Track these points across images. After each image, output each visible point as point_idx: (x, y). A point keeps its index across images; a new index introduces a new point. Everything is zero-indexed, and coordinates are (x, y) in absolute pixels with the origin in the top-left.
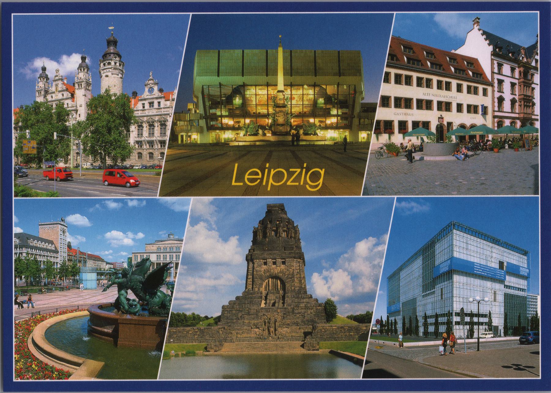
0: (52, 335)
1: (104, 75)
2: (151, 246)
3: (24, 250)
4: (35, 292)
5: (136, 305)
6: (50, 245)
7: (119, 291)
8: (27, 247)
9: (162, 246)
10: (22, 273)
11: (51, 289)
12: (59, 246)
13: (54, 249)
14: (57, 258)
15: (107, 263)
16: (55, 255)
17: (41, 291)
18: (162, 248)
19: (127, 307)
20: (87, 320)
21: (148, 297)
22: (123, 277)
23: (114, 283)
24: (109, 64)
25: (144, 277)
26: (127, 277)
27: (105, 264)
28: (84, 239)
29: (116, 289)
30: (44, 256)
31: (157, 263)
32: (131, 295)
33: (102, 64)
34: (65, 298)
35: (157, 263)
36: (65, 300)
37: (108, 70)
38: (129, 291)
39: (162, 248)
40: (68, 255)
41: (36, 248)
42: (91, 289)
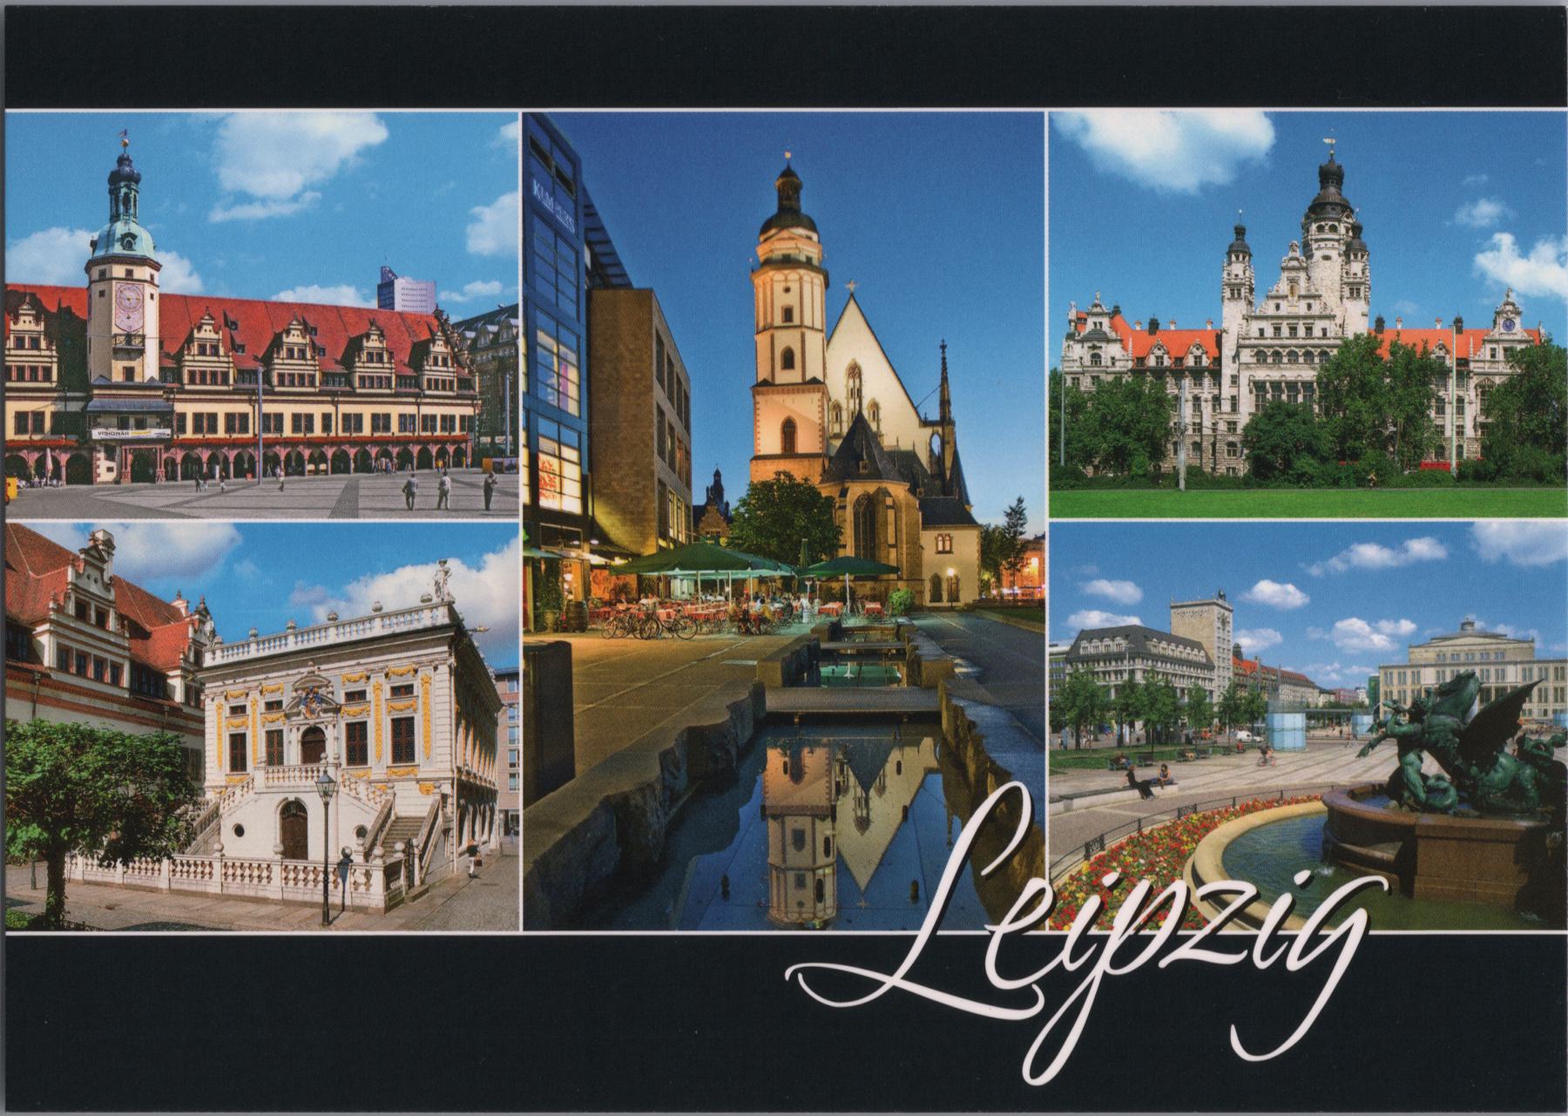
1: (1318, 255)
3: (1139, 665)
5: (1445, 791)
7: (1402, 755)
8: (1147, 656)
9: (1448, 651)
10: (1138, 715)
12: (1214, 654)
15: (1322, 692)
16: (1206, 674)
19: (1422, 795)
20: (1322, 823)
21: (1474, 770)
22: (1411, 721)
23: (1385, 737)
24: (1334, 229)
25: (1463, 720)
26: (1421, 721)
29: (1395, 750)
31: (1497, 690)
32: (1430, 766)
33: (1314, 226)
34: (1238, 772)
35: (1497, 690)
37: (1330, 244)
38: (1426, 755)
42: (1294, 750)
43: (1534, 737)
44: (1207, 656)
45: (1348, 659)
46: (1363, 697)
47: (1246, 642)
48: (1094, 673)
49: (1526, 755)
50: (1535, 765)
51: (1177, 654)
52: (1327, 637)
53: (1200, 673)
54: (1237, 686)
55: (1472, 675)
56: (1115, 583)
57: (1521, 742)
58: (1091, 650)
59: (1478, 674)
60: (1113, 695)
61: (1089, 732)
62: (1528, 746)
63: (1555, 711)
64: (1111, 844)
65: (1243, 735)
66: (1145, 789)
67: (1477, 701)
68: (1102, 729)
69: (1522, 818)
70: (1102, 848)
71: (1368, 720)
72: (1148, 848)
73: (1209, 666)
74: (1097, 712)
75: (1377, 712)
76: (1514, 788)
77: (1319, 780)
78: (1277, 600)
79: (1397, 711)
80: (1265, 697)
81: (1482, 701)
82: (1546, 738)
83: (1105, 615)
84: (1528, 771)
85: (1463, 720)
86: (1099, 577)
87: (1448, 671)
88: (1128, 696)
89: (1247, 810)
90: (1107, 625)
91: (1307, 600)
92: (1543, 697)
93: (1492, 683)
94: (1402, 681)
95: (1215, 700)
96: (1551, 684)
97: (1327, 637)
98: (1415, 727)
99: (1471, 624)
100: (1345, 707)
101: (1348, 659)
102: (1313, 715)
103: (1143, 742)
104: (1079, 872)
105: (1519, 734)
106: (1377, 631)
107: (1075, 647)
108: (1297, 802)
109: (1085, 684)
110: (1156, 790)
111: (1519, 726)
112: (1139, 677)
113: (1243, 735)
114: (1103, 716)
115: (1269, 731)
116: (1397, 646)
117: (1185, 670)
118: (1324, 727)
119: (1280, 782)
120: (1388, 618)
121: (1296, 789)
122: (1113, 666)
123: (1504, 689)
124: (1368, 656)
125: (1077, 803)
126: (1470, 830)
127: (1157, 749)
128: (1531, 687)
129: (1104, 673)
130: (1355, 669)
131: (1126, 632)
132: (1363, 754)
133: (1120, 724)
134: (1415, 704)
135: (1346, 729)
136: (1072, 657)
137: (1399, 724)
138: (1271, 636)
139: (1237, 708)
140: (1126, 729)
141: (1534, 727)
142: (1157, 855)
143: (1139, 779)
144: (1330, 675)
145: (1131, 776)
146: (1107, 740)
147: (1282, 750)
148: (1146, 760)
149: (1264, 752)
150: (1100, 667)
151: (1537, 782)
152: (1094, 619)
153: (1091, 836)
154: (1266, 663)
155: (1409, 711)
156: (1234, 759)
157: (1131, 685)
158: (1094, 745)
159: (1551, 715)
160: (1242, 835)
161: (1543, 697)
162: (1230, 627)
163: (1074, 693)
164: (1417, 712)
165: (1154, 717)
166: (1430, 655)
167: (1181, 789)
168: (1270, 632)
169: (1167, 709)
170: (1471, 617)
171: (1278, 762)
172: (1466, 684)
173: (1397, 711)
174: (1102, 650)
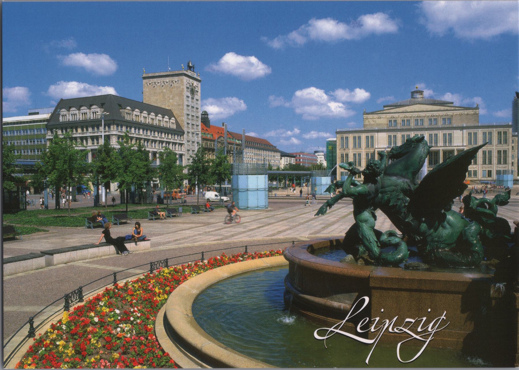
0: (207, 310)
2: (375, 116)
3: (114, 131)
5: (397, 246)
6: (166, 118)
7: (357, 213)
8: (120, 122)
10: (113, 177)
12: (184, 120)
13: (174, 127)
15: (284, 155)
17: (156, 214)
18: (399, 121)
19: (376, 250)
20: (284, 276)
21: (424, 226)
22: (366, 182)
23: (341, 196)
25: (413, 182)
26: (375, 182)
27: (278, 155)
28: (242, 106)
29: (351, 208)
30: (155, 141)
31: (445, 152)
32: (383, 223)
35: (445, 152)
36: (207, 233)
38: (379, 213)
39: (399, 121)
40: (203, 139)
41: (139, 126)
42: (257, 209)
43: (480, 197)
44: (177, 123)
45: (306, 125)
46: (321, 159)
47: (213, 110)
48: (72, 139)
49: (471, 213)
50: (479, 222)
51: (149, 121)
52: (287, 105)
53: (170, 138)
54: (205, 150)
56: (91, 56)
57: (467, 200)
58: (70, 118)
59: (427, 138)
60: (90, 160)
61: (68, 193)
62: (474, 204)
63: (498, 172)
64: (89, 296)
65: (211, 195)
66: (120, 244)
68: (80, 190)
69: (469, 270)
70: (81, 300)
71: (326, 181)
72: (123, 299)
73: (179, 132)
74: (75, 176)
75: (334, 173)
76: (461, 242)
77: (281, 237)
78: (241, 71)
79: (353, 173)
80: (231, 160)
81: (430, 163)
82: (490, 197)
83: (82, 86)
84: (474, 228)
85: (413, 182)
86: (76, 51)
87: (399, 135)
88: (103, 160)
89: (215, 263)
90: (84, 95)
91: (269, 71)
92: (487, 159)
93: (441, 146)
94: (357, 144)
95: (184, 163)
96: (494, 148)
97: (287, 105)
98: (369, 187)
99: (421, 92)
100: (303, 168)
101: (306, 125)
102: (274, 176)
103: (118, 202)
104: (60, 322)
105: (466, 193)
106: (334, 99)
107: (55, 115)
108: (261, 256)
109: (64, 149)
110: (130, 246)
111: (466, 186)
112: (114, 143)
113: (211, 195)
114: (80, 179)
115: (234, 192)
116: (352, 113)
117: (157, 136)
118: (285, 187)
119: (244, 238)
120: (344, 88)
122: (90, 132)
123: (452, 151)
124: (325, 122)
125: (57, 258)
126: (420, 281)
127: (131, 208)
128: (475, 150)
129: (82, 138)
130: (314, 134)
131: (103, 101)
132: (321, 212)
134: (368, 166)
135: (306, 189)
136: (52, 124)
137: (355, 185)
138: (238, 104)
139: (205, 170)
140: (102, 191)
141: (479, 187)
142: (132, 305)
143: (114, 236)
144: (290, 139)
145: (107, 233)
146: (86, 200)
147: (247, 209)
148: (121, 218)
149: (230, 211)
150: (78, 133)
151: (482, 236)
152: (72, 89)
153: (70, 288)
154: (231, 128)
155: (364, 173)
157: (107, 150)
158: (73, 205)
159: (494, 176)
160: (211, 287)
161: (487, 159)
162: (198, 96)
163: (54, 156)
164: (371, 174)
165: (128, 179)
166: (382, 120)
167: (152, 245)
168: (234, 100)
170: (420, 86)
171: (243, 220)
172: (416, 148)
173: (353, 173)
174: (80, 117)
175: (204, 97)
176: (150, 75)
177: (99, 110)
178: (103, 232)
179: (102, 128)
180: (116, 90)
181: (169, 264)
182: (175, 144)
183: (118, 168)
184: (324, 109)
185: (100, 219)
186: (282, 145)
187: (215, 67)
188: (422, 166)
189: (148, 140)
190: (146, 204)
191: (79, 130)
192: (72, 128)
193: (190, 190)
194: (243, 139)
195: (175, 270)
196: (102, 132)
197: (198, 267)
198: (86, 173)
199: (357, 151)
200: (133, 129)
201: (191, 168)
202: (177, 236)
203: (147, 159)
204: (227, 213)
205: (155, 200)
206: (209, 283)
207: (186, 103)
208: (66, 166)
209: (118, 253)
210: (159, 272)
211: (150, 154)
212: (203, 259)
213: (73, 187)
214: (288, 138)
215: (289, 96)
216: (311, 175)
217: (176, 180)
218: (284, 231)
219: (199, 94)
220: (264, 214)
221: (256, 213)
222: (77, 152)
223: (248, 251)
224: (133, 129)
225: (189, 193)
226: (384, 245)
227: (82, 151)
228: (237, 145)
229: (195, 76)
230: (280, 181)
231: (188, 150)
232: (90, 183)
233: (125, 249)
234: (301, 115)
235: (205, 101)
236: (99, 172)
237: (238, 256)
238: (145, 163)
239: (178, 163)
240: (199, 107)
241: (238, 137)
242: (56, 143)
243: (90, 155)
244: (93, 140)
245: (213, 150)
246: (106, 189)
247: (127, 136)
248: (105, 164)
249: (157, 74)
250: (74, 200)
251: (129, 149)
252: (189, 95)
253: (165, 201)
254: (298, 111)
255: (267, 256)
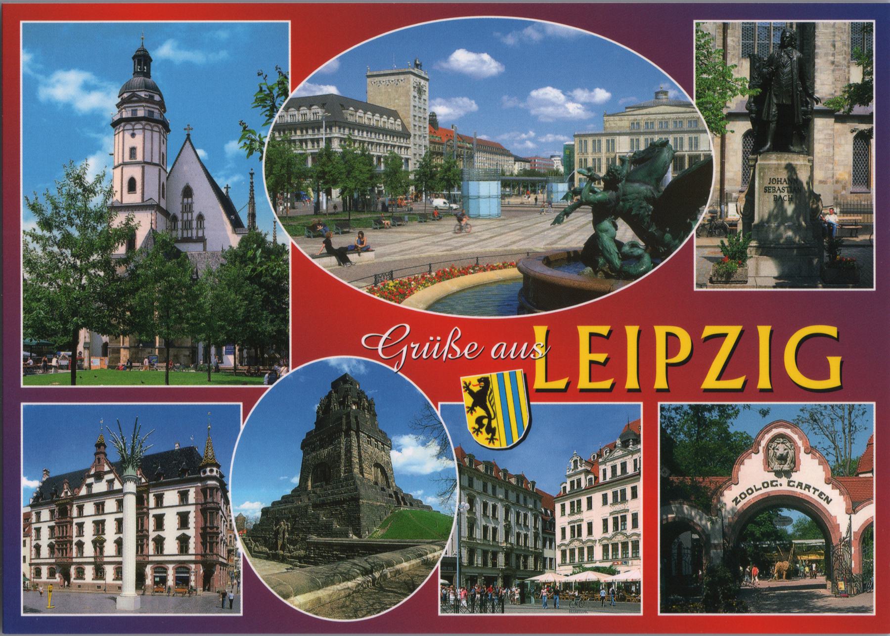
2: (617, 118)
3: (336, 133)
4: (366, 224)
5: (639, 258)
6: (392, 120)
7: (596, 222)
10: (335, 183)
11: (400, 219)
12: (410, 122)
13: (400, 129)
14: (407, 148)
15: (517, 159)
16: (402, 142)
17: (381, 223)
18: (642, 123)
19: (617, 262)
20: (518, 289)
21: (668, 237)
22: (606, 189)
23: (580, 204)
25: (657, 188)
26: (616, 189)
28: (474, 107)
29: (590, 217)
30: (380, 144)
31: (691, 157)
32: (625, 233)
35: (691, 157)
38: (620, 222)
39: (642, 123)
40: (431, 142)
41: (362, 127)
42: (489, 217)
44: (403, 124)
45: (542, 127)
47: (442, 111)
51: (373, 123)
52: (522, 105)
53: (395, 141)
54: (432, 154)
55: (665, 144)
59: (671, 142)
61: (286, 200)
65: (439, 202)
66: (342, 255)
67: (671, 169)
68: (299, 196)
71: (563, 187)
74: (294, 181)
75: (572, 180)
77: (514, 247)
78: (472, 69)
79: (592, 179)
80: (461, 165)
81: (675, 169)
85: (657, 188)
87: (642, 139)
88: (324, 165)
89: (443, 276)
91: (502, 69)
93: (686, 151)
94: (597, 148)
95: (411, 167)
97: (522, 105)
99: (666, 93)
100: (539, 174)
102: (508, 183)
103: (340, 209)
106: (572, 99)
108: (493, 268)
109: (281, 153)
110: (352, 257)
112: (336, 146)
113: (439, 202)
114: (300, 184)
115: (464, 199)
116: (591, 115)
117: (382, 139)
120: (583, 88)
121: (494, 255)
122: (310, 135)
123: (698, 156)
124: (562, 125)
129: (301, 141)
130: (550, 138)
131: (324, 101)
132: (558, 221)
133: (317, 192)
134: (609, 172)
135: (541, 197)
137: (594, 192)
139: (432, 176)
140: (323, 197)
143: (335, 246)
144: (525, 143)
145: (328, 244)
147: (478, 217)
148: (343, 227)
149: (460, 220)
150: (298, 135)
154: (462, 131)
155: (604, 179)
156: (431, 227)
157: (328, 153)
162: (426, 96)
164: (612, 181)
165: (351, 185)
166: (624, 123)
167: (377, 256)
169: (362, 177)
171: (474, 229)
172: (661, 152)
173: (592, 179)
174: (299, 118)
175: (432, 97)
176: (375, 73)
177: (319, 110)
178: (324, 242)
179: (322, 131)
180: (338, 88)
181: (394, 276)
182: (401, 147)
183: (341, 173)
184: (561, 110)
185: (320, 228)
186: (515, 148)
187: (445, 65)
188: (666, 171)
189: (372, 143)
190: (370, 212)
191: (299, 132)
192: (290, 130)
193: (417, 196)
194: (475, 143)
195: (401, 283)
196: (323, 134)
197: (425, 280)
198: (305, 179)
199: (596, 156)
200: (356, 131)
201: (417, 173)
202: (403, 246)
203: (371, 164)
204: (456, 222)
205: (380, 207)
206: (438, 297)
207: (413, 103)
208: (283, 171)
209: (340, 265)
210: (384, 285)
211: (375, 159)
212: (430, 272)
213: (292, 193)
214: (523, 142)
215: (524, 95)
216: (547, 182)
217: (401, 186)
218: (520, 241)
219: (427, 93)
220: (497, 223)
221: (488, 222)
222: (296, 156)
223: (480, 262)
224: (356, 131)
225: (416, 201)
226: (625, 257)
227: (301, 154)
228: (467, 148)
229: (423, 75)
230: (514, 187)
231: (415, 154)
232: (310, 189)
233: (347, 260)
234: (536, 117)
235: (433, 101)
236: (319, 178)
237: (468, 268)
238: (368, 168)
239: (403, 168)
240: (427, 108)
241: (469, 140)
242: (273, 146)
243: (310, 159)
244: (313, 143)
245: (441, 154)
246: (327, 195)
247: (349, 138)
248: (327, 169)
249: (382, 72)
250: (293, 207)
251: (352, 153)
252: (416, 95)
253: (390, 209)
254: (533, 112)
255: (500, 268)
